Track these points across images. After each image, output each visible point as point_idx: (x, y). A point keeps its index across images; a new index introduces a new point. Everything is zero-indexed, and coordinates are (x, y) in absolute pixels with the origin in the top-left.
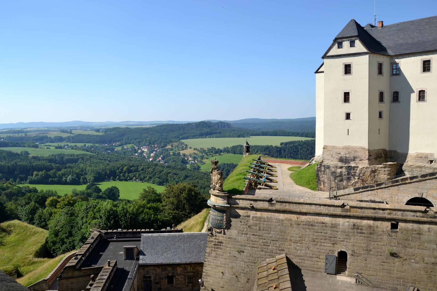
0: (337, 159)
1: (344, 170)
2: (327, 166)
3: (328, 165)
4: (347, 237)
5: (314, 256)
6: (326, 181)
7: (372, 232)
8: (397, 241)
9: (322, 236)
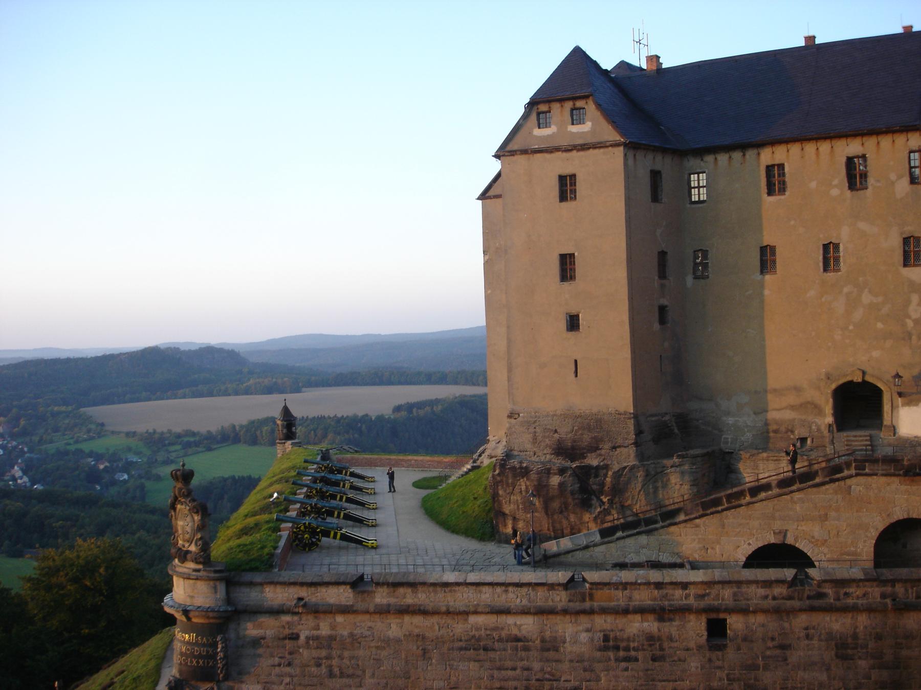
1: (568, 478)
2: (521, 468)
4: (587, 675)
7: (658, 653)
8: (728, 675)
9: (518, 680)
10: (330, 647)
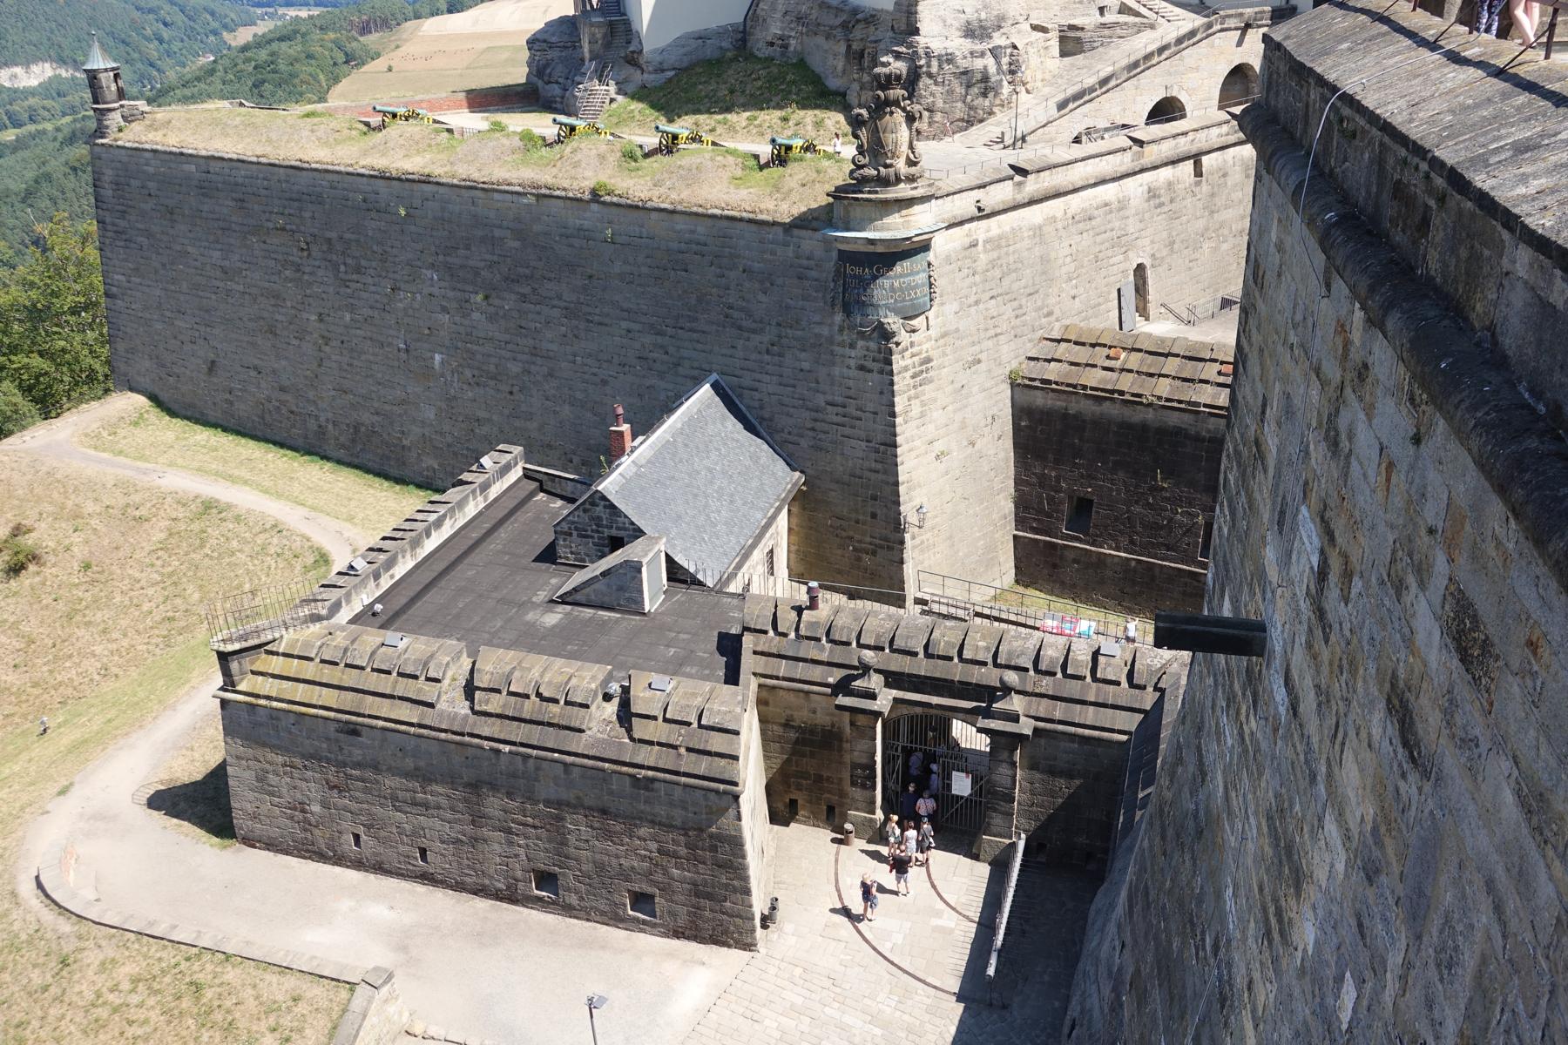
0: (958, 29)
1: (990, 62)
3: (949, 51)
5: (1101, 300)
6: (940, 104)
10: (999, 247)
